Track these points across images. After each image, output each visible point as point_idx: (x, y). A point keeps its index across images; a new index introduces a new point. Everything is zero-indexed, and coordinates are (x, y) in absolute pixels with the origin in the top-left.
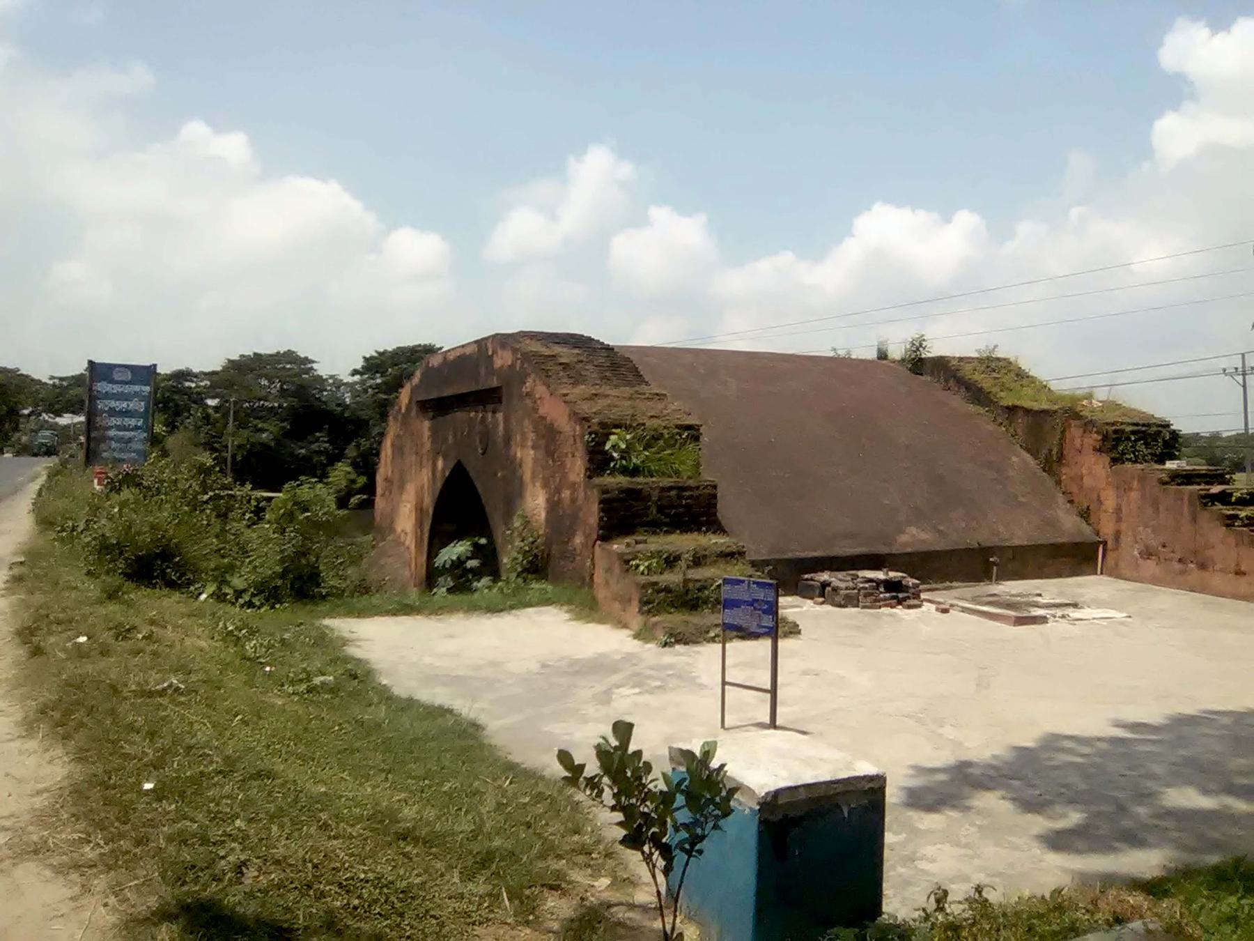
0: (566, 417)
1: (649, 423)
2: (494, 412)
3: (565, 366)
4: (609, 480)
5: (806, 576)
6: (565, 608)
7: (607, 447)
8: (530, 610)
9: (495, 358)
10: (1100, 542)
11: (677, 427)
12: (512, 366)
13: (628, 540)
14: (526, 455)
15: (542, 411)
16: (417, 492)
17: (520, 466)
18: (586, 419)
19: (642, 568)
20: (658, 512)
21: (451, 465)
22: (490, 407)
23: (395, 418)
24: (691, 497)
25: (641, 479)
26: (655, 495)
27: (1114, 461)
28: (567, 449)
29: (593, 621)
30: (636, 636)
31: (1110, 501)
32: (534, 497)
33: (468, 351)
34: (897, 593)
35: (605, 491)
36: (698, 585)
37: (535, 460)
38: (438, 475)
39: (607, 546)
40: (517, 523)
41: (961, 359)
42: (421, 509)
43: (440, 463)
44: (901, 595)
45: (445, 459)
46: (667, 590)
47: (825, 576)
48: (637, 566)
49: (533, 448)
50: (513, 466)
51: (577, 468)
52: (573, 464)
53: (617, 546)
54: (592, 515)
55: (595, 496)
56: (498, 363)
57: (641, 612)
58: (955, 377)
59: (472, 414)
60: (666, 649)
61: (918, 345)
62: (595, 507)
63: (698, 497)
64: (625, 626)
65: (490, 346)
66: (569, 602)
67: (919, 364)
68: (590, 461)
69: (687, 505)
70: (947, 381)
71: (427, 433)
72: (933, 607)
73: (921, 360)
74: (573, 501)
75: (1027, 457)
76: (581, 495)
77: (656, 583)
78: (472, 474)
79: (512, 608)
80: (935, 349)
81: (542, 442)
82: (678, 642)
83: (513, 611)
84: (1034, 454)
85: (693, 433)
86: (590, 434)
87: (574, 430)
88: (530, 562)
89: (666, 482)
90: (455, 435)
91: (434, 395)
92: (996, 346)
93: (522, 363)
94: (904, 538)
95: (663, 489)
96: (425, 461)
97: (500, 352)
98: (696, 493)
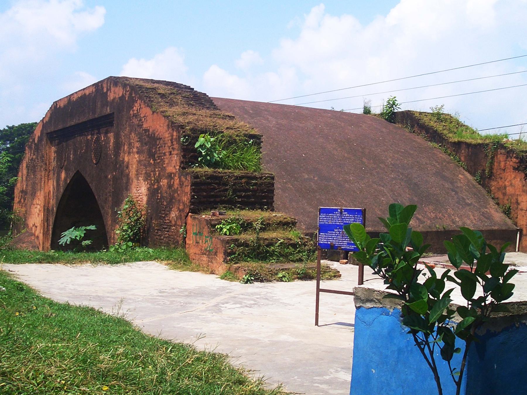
0: (166, 128)
1: (226, 133)
2: (106, 133)
3: (163, 96)
4: (196, 169)
7: (196, 146)
11: (245, 135)
12: (122, 98)
14: (132, 160)
15: (144, 126)
16: (45, 197)
17: (127, 167)
18: (182, 127)
19: (225, 230)
21: (72, 174)
22: (103, 130)
23: (30, 148)
24: (255, 184)
26: (231, 182)
29: (187, 270)
30: (222, 278)
32: (138, 187)
33: (87, 92)
35: (196, 177)
37: (139, 162)
41: (421, 113)
42: (48, 209)
43: (63, 175)
45: (66, 173)
48: (221, 229)
49: (138, 153)
52: (171, 160)
53: (205, 216)
55: (188, 182)
56: (111, 96)
57: (226, 261)
58: (418, 124)
59: (89, 137)
60: (248, 285)
61: (392, 104)
62: (188, 189)
63: (261, 184)
64: (212, 273)
65: (105, 85)
66: (168, 258)
67: (393, 117)
68: (184, 156)
70: (412, 127)
71: (53, 155)
73: (394, 113)
74: (170, 186)
76: (177, 182)
77: (237, 240)
78: (88, 180)
79: (126, 261)
80: (402, 108)
81: (146, 148)
82: (257, 280)
85: (257, 139)
86: (185, 136)
87: (172, 136)
88: (135, 234)
89: (237, 173)
90: (75, 151)
91: (60, 127)
93: (131, 94)
95: (237, 178)
96: (51, 175)
97: (112, 89)
98: (259, 181)
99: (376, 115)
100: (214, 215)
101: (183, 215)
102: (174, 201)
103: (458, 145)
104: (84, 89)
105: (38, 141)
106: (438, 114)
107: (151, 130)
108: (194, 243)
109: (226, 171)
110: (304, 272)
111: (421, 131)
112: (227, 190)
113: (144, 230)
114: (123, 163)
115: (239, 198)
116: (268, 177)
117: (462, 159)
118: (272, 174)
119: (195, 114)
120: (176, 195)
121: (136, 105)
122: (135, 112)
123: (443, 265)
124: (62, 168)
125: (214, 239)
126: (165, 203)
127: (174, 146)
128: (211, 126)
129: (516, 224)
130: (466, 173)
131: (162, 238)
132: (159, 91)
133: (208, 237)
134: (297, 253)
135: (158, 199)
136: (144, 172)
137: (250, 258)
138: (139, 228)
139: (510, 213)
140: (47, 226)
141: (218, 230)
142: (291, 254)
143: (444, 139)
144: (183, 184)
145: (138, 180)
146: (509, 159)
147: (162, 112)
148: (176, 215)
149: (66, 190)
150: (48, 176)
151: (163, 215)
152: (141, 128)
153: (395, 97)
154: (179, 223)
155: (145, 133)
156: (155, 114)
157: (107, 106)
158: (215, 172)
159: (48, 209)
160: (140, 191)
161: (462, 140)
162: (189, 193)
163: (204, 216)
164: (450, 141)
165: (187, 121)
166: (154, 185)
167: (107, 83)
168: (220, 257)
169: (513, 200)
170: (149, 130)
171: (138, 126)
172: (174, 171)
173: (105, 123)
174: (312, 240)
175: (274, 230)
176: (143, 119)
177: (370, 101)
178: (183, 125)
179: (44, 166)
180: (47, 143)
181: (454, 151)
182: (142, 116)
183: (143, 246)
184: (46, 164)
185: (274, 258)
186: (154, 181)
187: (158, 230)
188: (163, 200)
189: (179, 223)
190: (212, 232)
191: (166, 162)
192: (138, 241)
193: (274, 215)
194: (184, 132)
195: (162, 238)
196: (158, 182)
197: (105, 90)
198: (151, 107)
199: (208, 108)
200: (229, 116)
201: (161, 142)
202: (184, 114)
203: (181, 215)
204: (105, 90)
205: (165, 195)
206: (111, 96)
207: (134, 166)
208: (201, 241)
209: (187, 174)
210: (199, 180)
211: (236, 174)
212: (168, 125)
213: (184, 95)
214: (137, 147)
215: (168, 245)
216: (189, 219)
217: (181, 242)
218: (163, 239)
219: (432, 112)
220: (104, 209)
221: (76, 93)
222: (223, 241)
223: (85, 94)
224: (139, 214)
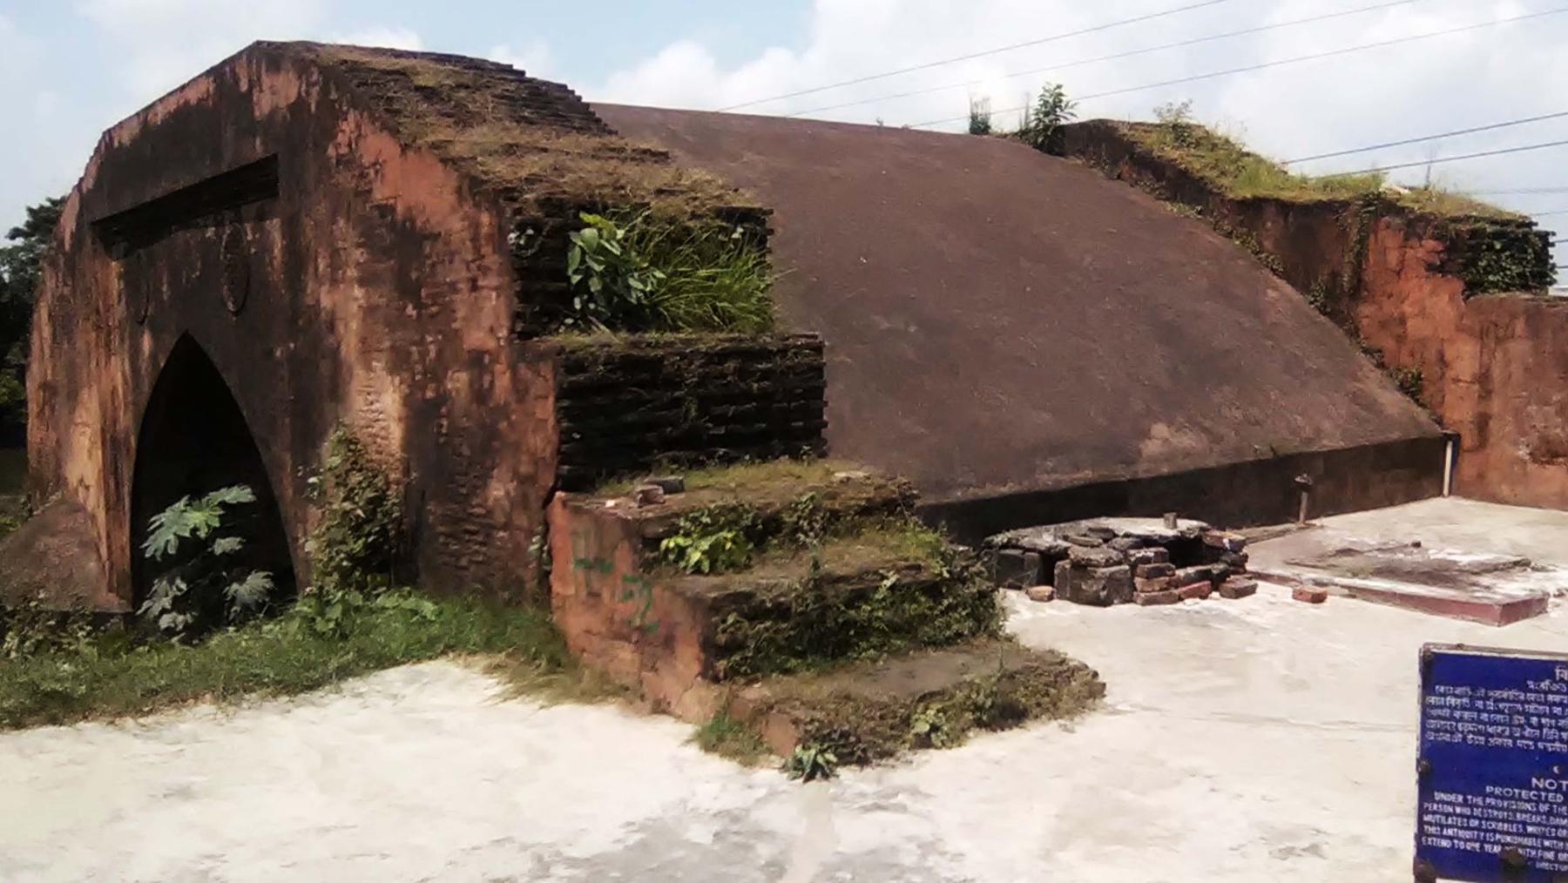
0: (451, 198)
2: (261, 217)
3: (429, 94)
4: (569, 338)
5: (1000, 539)
6: (482, 661)
8: (393, 675)
10: (1448, 437)
11: (719, 213)
12: (299, 106)
13: (639, 486)
14: (346, 303)
15: (380, 194)
17: (332, 327)
18: (509, 193)
20: (703, 411)
21: (170, 341)
22: (250, 210)
23: (53, 264)
24: (766, 375)
25: (652, 336)
27: (1473, 287)
28: (458, 273)
29: (567, 695)
31: (1465, 357)
32: (371, 392)
33: (193, 96)
34: (1202, 566)
36: (844, 588)
37: (369, 311)
38: (144, 366)
39: (588, 503)
40: (331, 457)
41: (1133, 126)
42: (114, 440)
43: (147, 343)
44: (1217, 568)
45: (156, 338)
46: (780, 612)
47: (1045, 538)
48: (681, 552)
49: (362, 282)
50: (314, 331)
51: (487, 320)
52: (475, 308)
54: (539, 426)
56: (264, 104)
57: (711, 676)
59: (210, 233)
61: (1053, 104)
62: (546, 410)
64: (660, 708)
66: (488, 646)
67: (1054, 137)
68: (524, 296)
69: (764, 396)
71: (116, 285)
72: (1285, 592)
73: (1062, 129)
74: (481, 395)
75: (1288, 289)
76: (503, 381)
78: (217, 360)
79: (344, 672)
80: (1082, 110)
81: (385, 266)
82: (845, 760)
83: (352, 684)
84: (1304, 288)
86: (521, 228)
87: (476, 226)
91: (127, 203)
92: (1186, 105)
93: (325, 92)
94: (1151, 447)
96: (116, 342)
97: (266, 81)
99: (1005, 136)
100: (647, 499)
101: (532, 497)
102: (496, 444)
103: (1253, 208)
104: (183, 88)
105: (72, 246)
106: (1175, 127)
107: (400, 209)
108: (583, 593)
109: (669, 336)
110: (999, 700)
111: (1139, 174)
112: (677, 403)
113: (400, 533)
114: (318, 314)
115: (717, 425)
116: (807, 346)
117: (1268, 244)
118: (815, 337)
119: (545, 150)
120: (503, 425)
121: (344, 126)
122: (344, 150)
123: (1349, 588)
124: (142, 323)
125: (656, 591)
126: (466, 451)
127: (487, 262)
128: (603, 186)
129: (1440, 422)
130: (1282, 283)
131: (464, 562)
132: (421, 81)
133: (634, 580)
134: (942, 613)
135: (440, 434)
136: (387, 344)
137: (801, 655)
138: (383, 527)
139: (1420, 390)
141: (671, 557)
142: (923, 619)
143: (1210, 192)
144: (527, 391)
145: (369, 369)
146: (1414, 242)
147: (434, 146)
148: (507, 493)
149: (156, 389)
150: (108, 344)
151: (464, 491)
152: (365, 202)
153: (1059, 87)
154: (522, 520)
155: (383, 216)
156: (410, 154)
157: (254, 137)
158: (635, 345)
159: (114, 440)
160: (377, 406)
161: (1262, 192)
162: (552, 421)
163: (610, 503)
164: (1231, 196)
165: (523, 174)
166: (424, 388)
167: (250, 62)
168: (688, 658)
169: (1431, 355)
170: (393, 209)
171: (358, 194)
172: (491, 344)
173: (250, 187)
174: (978, 557)
175: (854, 532)
176: (372, 171)
177: (986, 100)
178: (513, 190)
179: (93, 318)
180: (95, 251)
181: (1241, 224)
182: (366, 161)
183: (400, 583)
184: (98, 312)
185: (874, 640)
186: (425, 374)
187: (447, 535)
188: (457, 441)
189: (522, 520)
190: (648, 566)
191: (460, 314)
192: (382, 568)
193: (841, 475)
194: (518, 212)
195: (464, 562)
196: (439, 380)
197: (244, 87)
198: (395, 132)
199: (580, 130)
200: (654, 154)
201: (440, 245)
202: (510, 149)
203: (525, 497)
204: (244, 87)
205: (464, 422)
206: (264, 104)
207: (354, 325)
208: (606, 595)
209: (542, 356)
210: (581, 377)
211: (702, 347)
212: (459, 191)
213: (498, 92)
214: (359, 264)
215: (488, 592)
216: (558, 514)
217: (531, 585)
218: (465, 568)
219: (1157, 122)
221: (161, 100)
222: (696, 602)
223: (187, 103)
224: (379, 481)
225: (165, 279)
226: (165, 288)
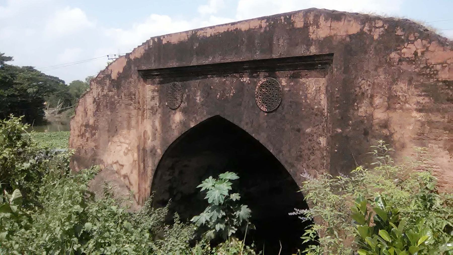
9: (311, 29)
16: (139, 138)
33: (244, 28)
42: (144, 149)
49: (419, 111)
59: (246, 79)
104: (233, 24)
140: (144, 167)
150: (143, 115)
180: (139, 81)
184: (139, 103)
220: (293, 166)
221: (211, 28)
225: (199, 94)
226: (198, 98)
